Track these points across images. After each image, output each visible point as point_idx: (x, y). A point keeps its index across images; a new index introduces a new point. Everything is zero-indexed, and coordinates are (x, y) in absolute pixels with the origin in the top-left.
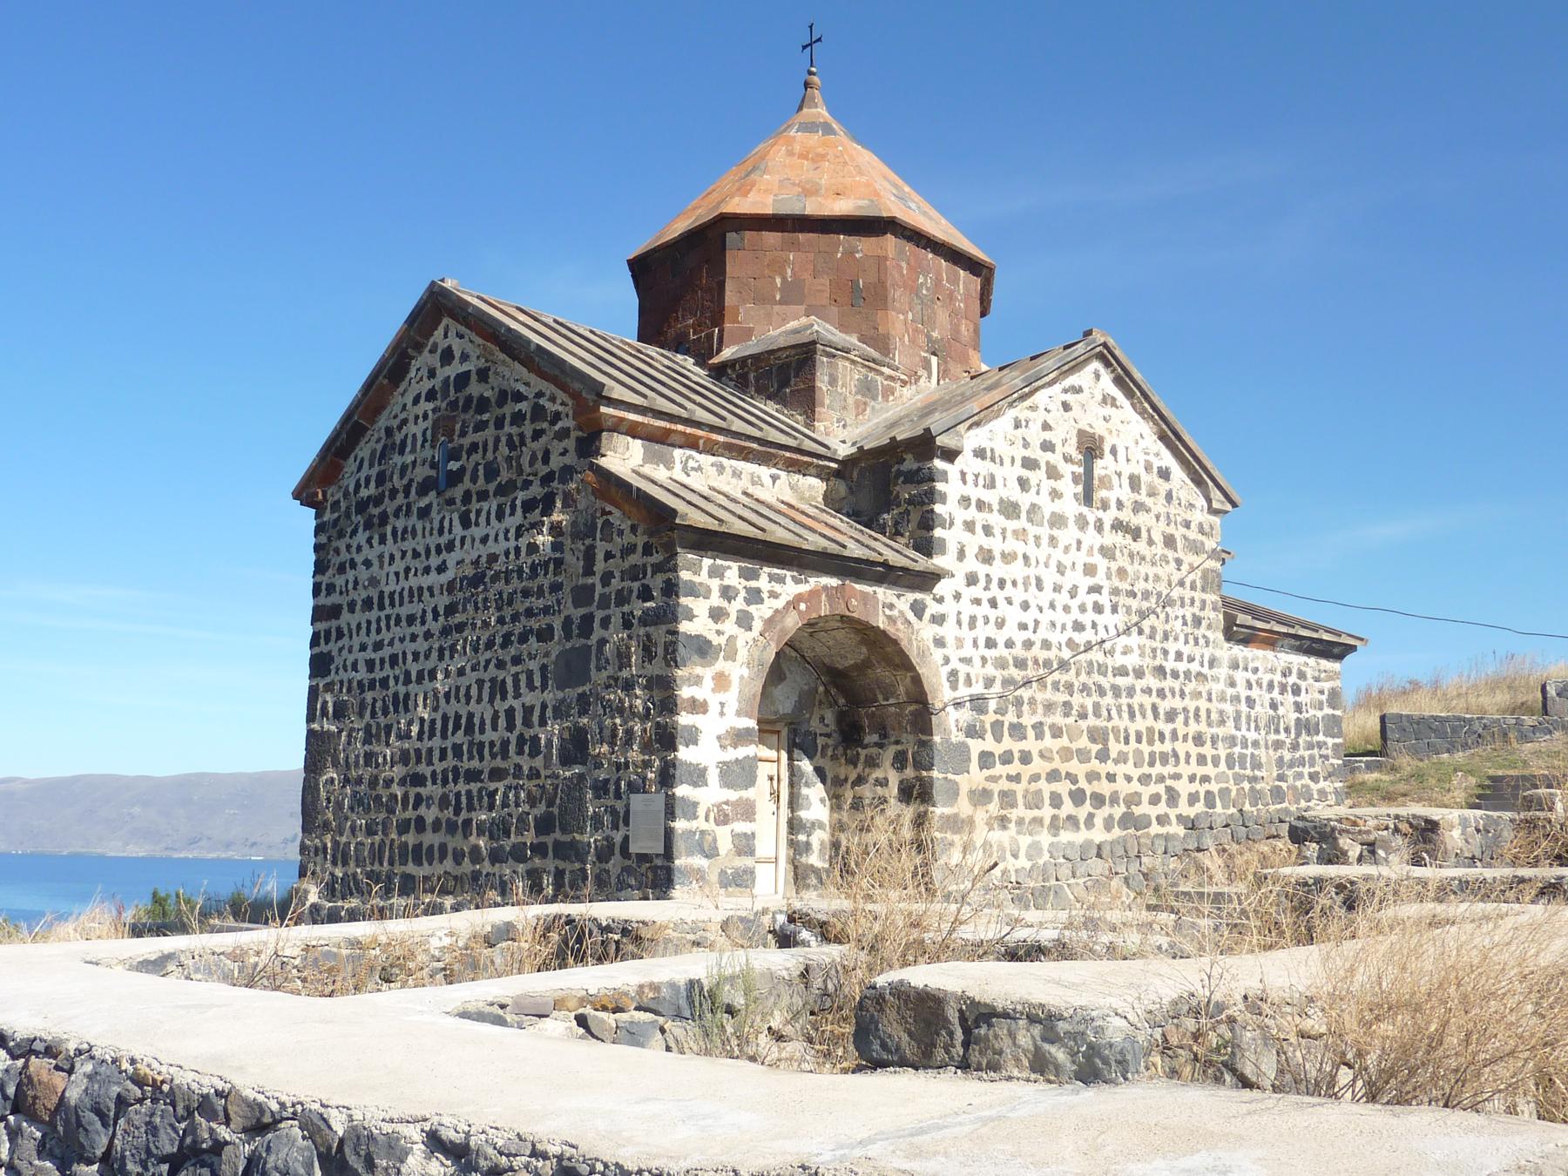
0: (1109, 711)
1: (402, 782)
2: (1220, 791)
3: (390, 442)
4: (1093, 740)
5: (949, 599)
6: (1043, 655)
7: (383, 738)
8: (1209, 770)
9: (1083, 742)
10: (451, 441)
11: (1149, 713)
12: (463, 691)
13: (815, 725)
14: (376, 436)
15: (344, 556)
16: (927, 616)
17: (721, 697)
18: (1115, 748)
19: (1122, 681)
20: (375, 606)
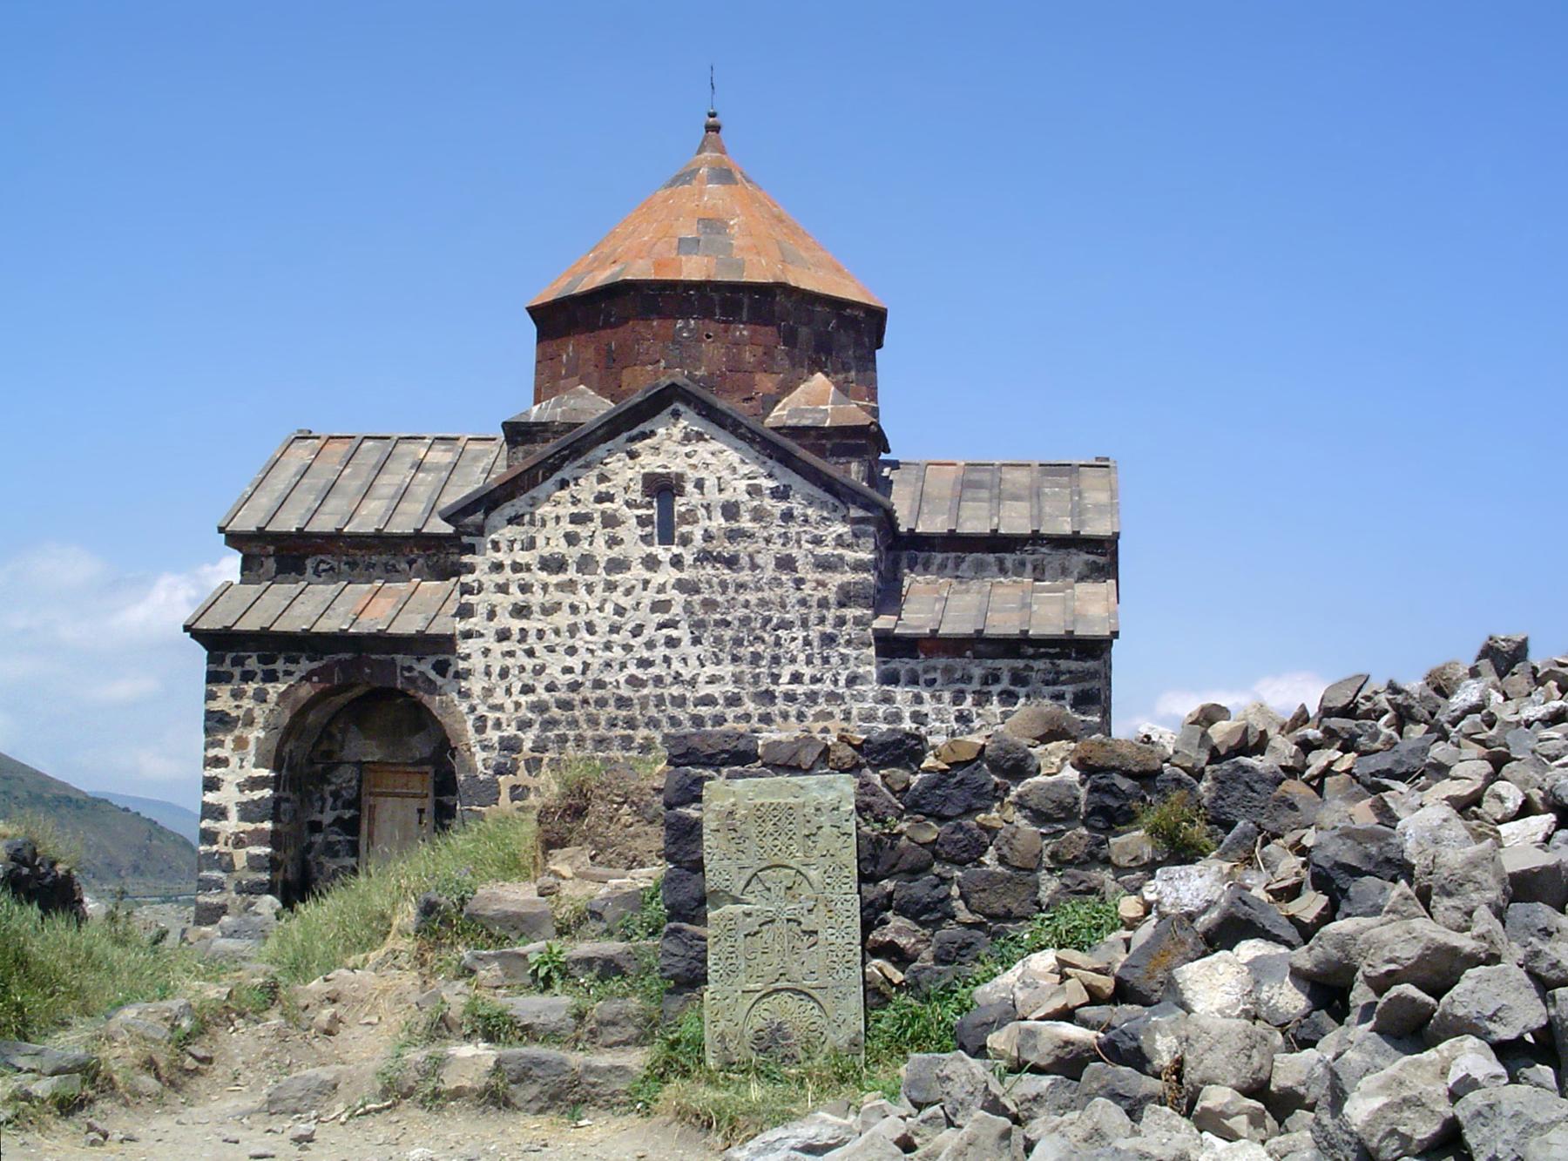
6: (593, 695)
16: (451, 670)
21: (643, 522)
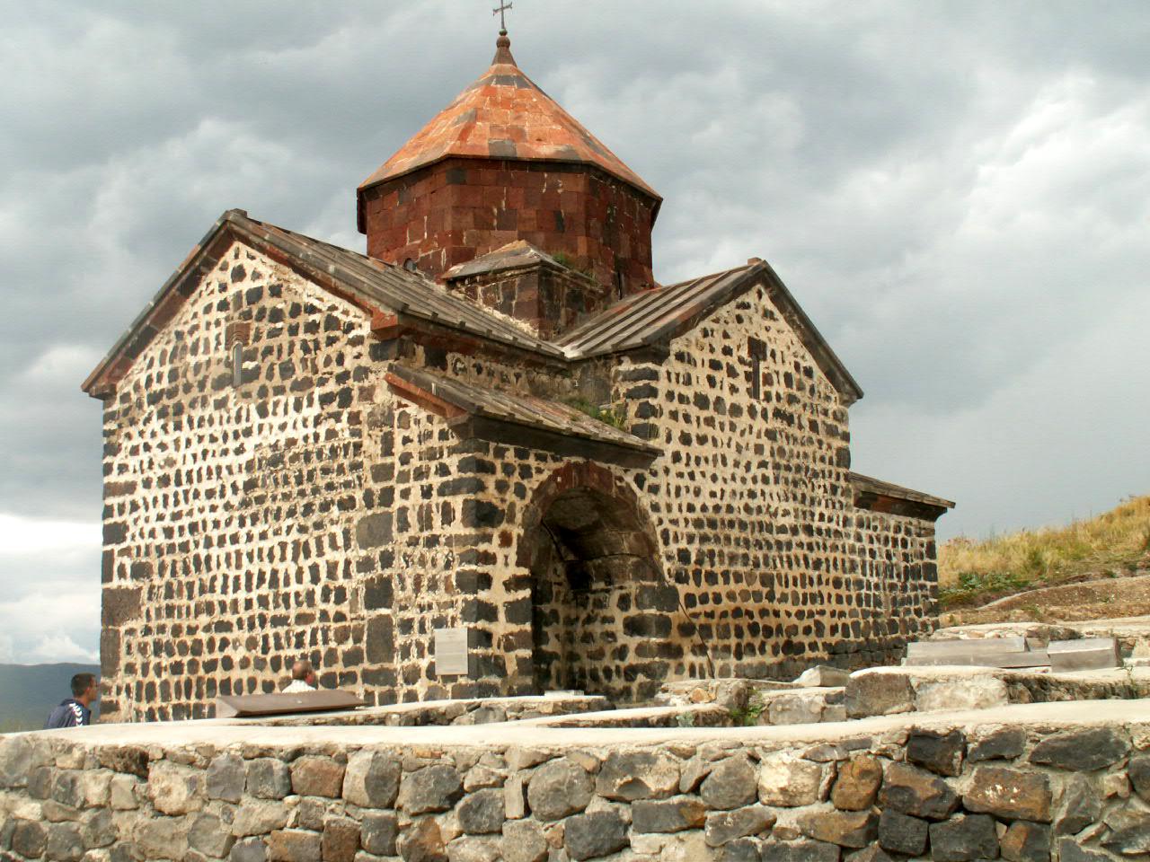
0: (774, 561)
1: (207, 629)
2: (853, 623)
3: (181, 344)
4: (763, 584)
5: (661, 473)
6: (728, 517)
7: (185, 593)
8: (845, 607)
9: (757, 586)
10: (246, 344)
11: (802, 562)
12: (265, 553)
13: (552, 577)
14: (166, 339)
15: (137, 441)
17: (506, 551)
18: (778, 590)
19: (783, 537)
20: (172, 482)
21: (748, 377)
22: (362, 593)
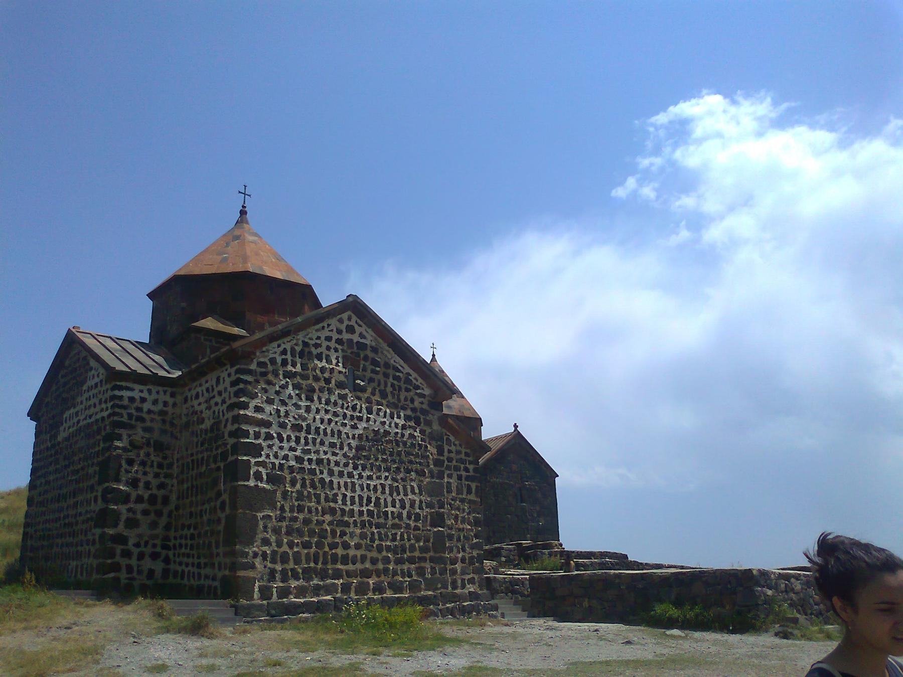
12: (372, 487)
14: (295, 341)
22: (429, 516)
